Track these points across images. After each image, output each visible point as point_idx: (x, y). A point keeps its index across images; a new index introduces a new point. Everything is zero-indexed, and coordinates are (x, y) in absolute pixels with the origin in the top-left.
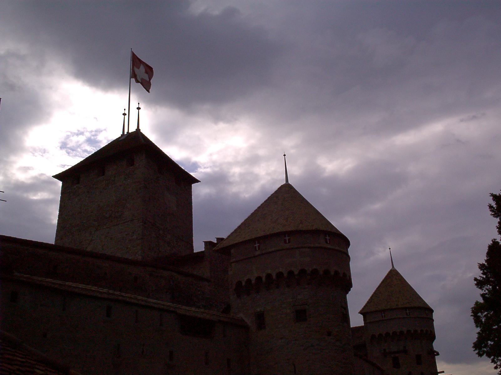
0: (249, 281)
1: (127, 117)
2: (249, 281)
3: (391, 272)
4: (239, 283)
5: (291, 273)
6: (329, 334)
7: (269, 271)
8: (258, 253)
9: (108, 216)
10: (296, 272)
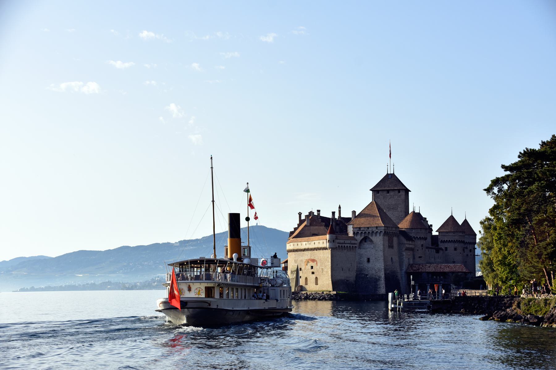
0: (444, 240)
1: (389, 167)
2: (444, 240)
4: (442, 240)
5: (454, 240)
6: (461, 253)
8: (447, 235)
9: (392, 208)
10: (456, 240)
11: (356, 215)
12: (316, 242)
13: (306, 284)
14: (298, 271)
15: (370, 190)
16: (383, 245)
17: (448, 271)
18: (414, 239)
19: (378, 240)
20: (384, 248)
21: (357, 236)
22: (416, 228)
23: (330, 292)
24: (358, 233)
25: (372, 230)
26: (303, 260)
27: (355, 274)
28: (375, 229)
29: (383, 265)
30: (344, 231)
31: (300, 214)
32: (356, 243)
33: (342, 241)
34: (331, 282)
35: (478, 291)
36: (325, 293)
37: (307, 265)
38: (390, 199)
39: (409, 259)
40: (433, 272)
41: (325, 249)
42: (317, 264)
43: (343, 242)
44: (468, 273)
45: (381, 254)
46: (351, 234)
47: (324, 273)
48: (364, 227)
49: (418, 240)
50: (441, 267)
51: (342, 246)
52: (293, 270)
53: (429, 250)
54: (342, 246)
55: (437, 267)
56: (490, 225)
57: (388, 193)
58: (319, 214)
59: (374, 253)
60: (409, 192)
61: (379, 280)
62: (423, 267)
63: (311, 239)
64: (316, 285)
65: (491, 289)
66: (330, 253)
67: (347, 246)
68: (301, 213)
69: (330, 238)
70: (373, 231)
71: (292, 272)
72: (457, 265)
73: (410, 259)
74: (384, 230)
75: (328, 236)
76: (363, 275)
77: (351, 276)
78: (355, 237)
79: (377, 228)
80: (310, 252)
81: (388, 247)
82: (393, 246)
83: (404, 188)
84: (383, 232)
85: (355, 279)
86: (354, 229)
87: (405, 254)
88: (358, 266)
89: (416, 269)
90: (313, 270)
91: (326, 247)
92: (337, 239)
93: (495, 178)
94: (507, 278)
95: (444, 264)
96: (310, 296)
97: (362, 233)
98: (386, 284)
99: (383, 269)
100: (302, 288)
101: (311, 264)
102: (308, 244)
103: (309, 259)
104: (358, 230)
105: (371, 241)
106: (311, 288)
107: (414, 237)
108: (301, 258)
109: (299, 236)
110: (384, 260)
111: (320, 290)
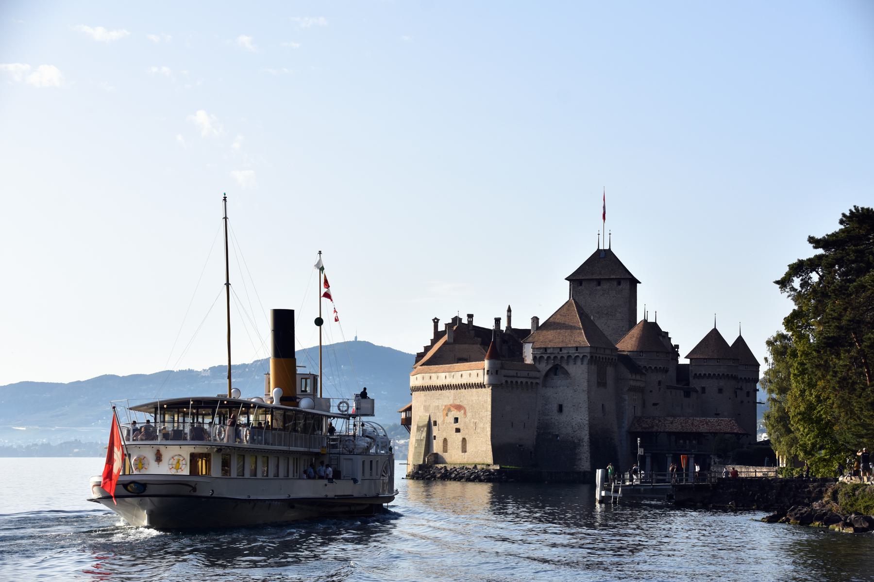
0: (700, 374)
2: (700, 374)
3: (738, 337)
4: (696, 374)
5: (719, 374)
6: (730, 399)
7: (710, 373)
8: (705, 364)
11: (540, 325)
12: (465, 374)
13: (445, 450)
14: (430, 426)
15: (566, 279)
16: (588, 381)
17: (706, 431)
18: (644, 371)
19: (579, 372)
20: (589, 386)
21: (539, 364)
23: (489, 465)
24: (541, 357)
25: (568, 353)
26: (440, 405)
27: (535, 433)
28: (574, 352)
29: (587, 419)
30: (518, 354)
31: (436, 321)
33: (512, 373)
34: (490, 447)
35: (762, 469)
36: (479, 467)
37: (447, 415)
38: (601, 295)
39: (635, 407)
40: (678, 432)
41: (481, 386)
42: (465, 413)
43: (515, 375)
44: (744, 434)
45: (584, 397)
46: (529, 360)
47: (478, 430)
48: (553, 348)
49: (652, 372)
50: (692, 424)
51: (512, 382)
52: (421, 425)
53: (671, 391)
54: (512, 382)
55: (686, 423)
56: (785, 347)
57: (599, 284)
58: (470, 322)
59: (571, 396)
61: (579, 445)
62: (660, 423)
63: (456, 367)
64: (462, 452)
65: (785, 466)
66: (491, 394)
67: (522, 382)
68: (438, 320)
69: (491, 366)
70: (570, 354)
71: (419, 428)
72: (722, 420)
73: (636, 408)
74: (591, 353)
75: (486, 363)
76: (550, 436)
77: (527, 436)
78: (537, 365)
79: (577, 350)
80: (453, 392)
82: (606, 383)
83: (631, 277)
84: (589, 357)
85: (535, 443)
86: (535, 350)
87: (627, 398)
88: (541, 418)
89: (647, 426)
90: (457, 426)
91: (482, 383)
92: (502, 368)
93: (795, 261)
94: (814, 445)
95: (698, 419)
96: (451, 473)
97: (549, 357)
98: (591, 452)
99: (587, 426)
100: (437, 459)
101: (455, 413)
102: (450, 377)
103: (451, 405)
104: (541, 353)
105: (566, 373)
106: (454, 457)
108: (436, 403)
109: (432, 362)
111: (470, 461)
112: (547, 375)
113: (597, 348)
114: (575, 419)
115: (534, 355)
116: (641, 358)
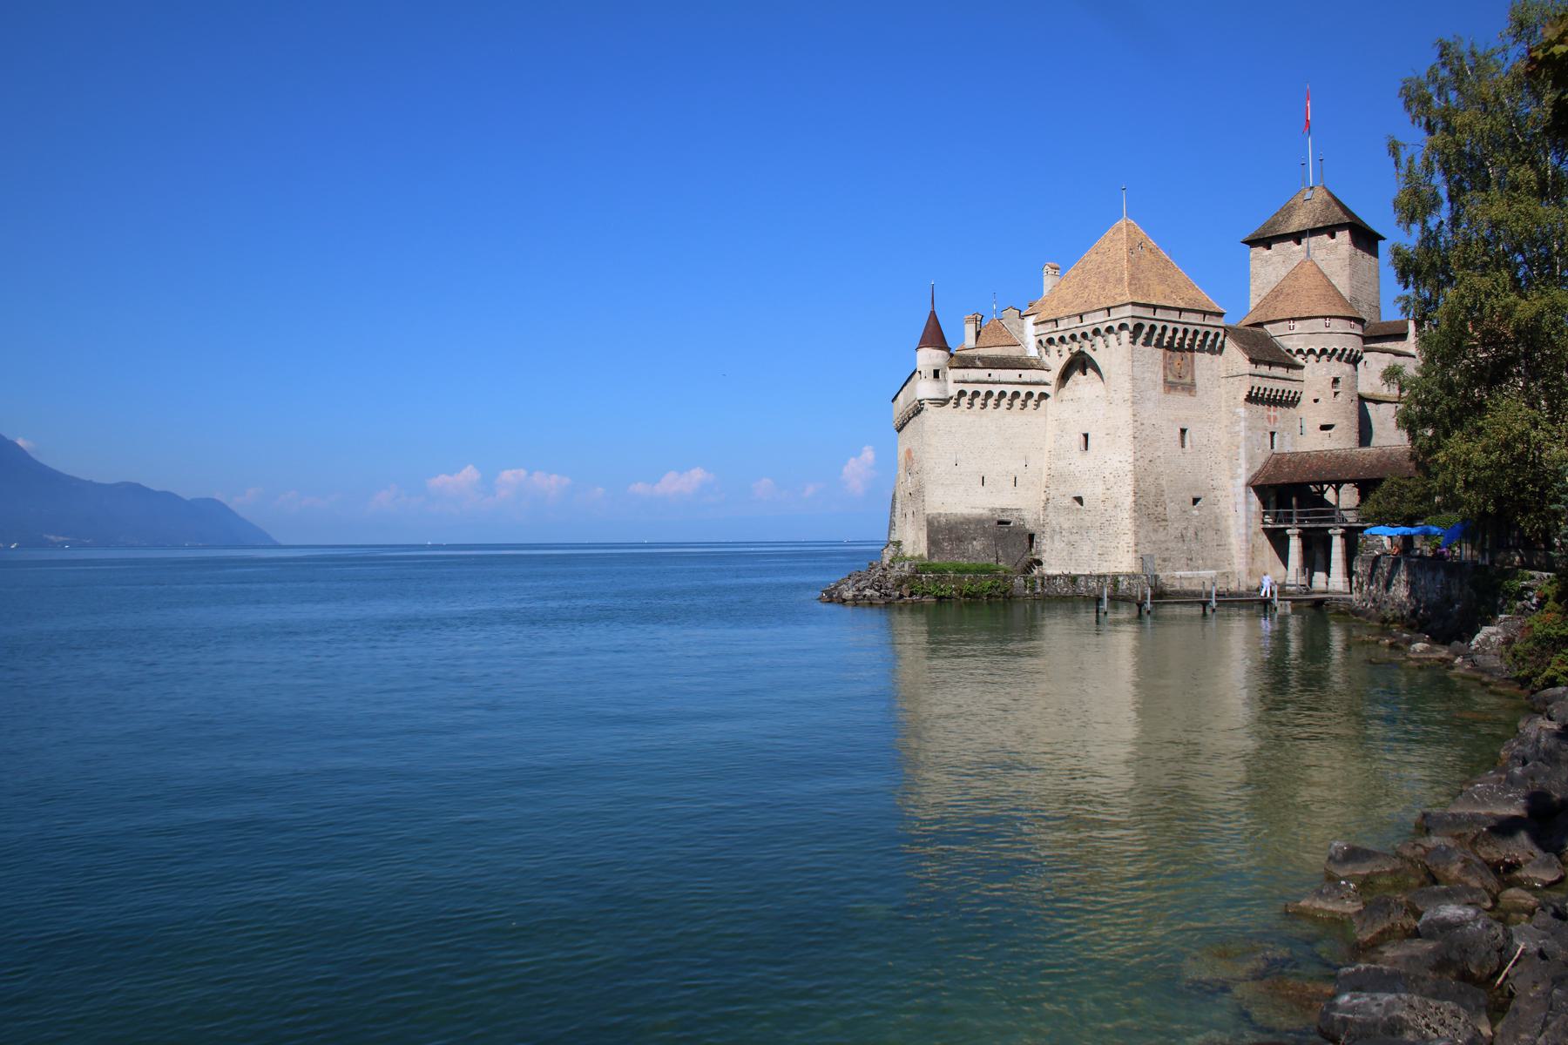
16: (1133, 379)
18: (1299, 359)
22: (1305, 315)
24: (1050, 341)
29: (1131, 460)
32: (1047, 380)
39: (1272, 434)
43: (986, 378)
45: (1124, 414)
48: (1069, 317)
59: (1104, 415)
60: (1380, 242)
73: (1276, 435)
78: (1045, 358)
81: (1160, 388)
84: (1131, 328)
99: (1129, 474)
105: (1097, 370)
107: (1300, 351)
110: (1134, 438)
112: (1065, 376)
113: (1155, 307)
114: (1109, 462)
115: (1039, 338)
116: (1291, 332)
